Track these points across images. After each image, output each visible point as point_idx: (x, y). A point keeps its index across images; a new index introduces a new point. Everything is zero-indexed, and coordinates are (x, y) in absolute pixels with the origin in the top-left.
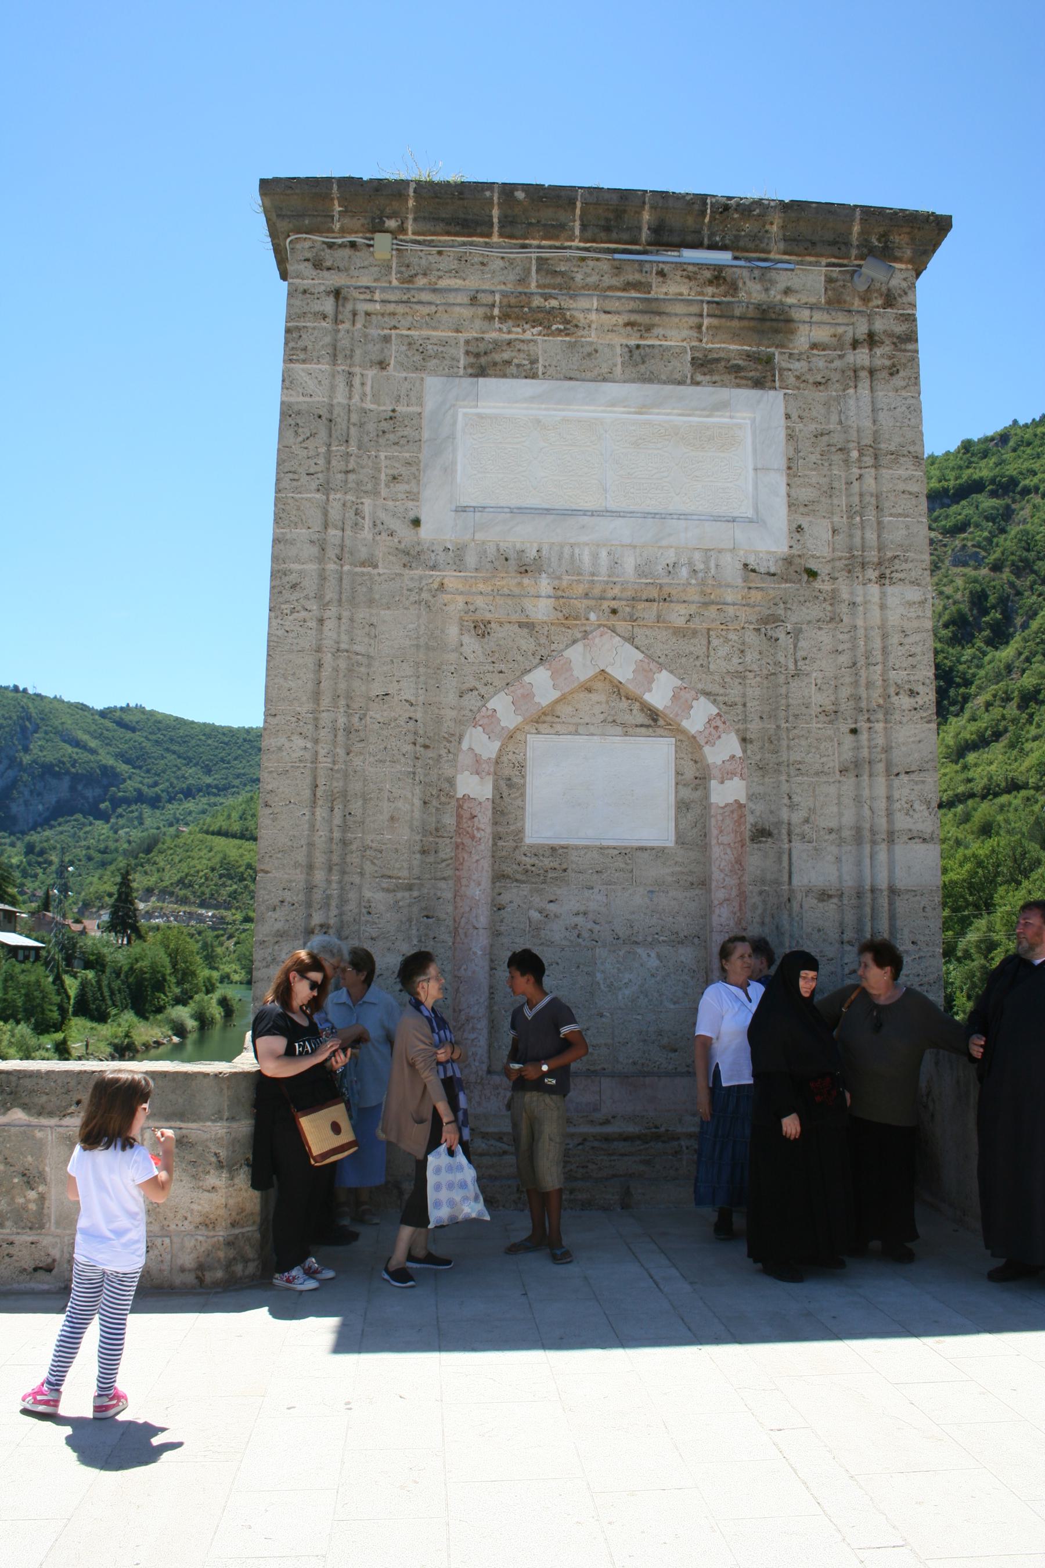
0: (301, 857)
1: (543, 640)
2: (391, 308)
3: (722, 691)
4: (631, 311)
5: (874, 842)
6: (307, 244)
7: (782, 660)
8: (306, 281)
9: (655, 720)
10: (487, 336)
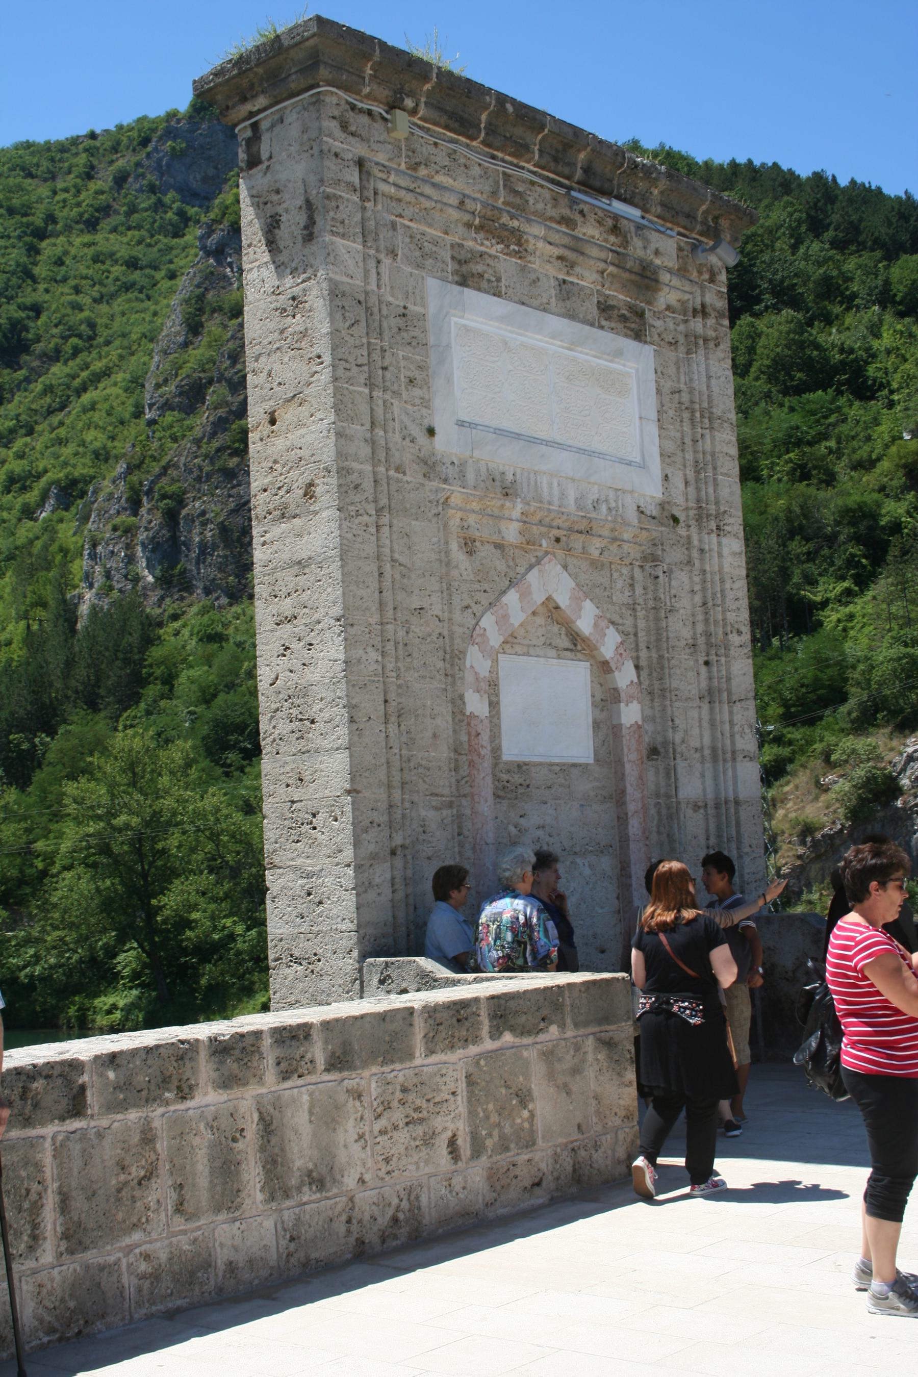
0: (382, 774)
1: (511, 563)
2: (402, 193)
3: (621, 621)
4: (565, 246)
5: (725, 760)
6: (334, 100)
7: (662, 596)
8: (336, 143)
9: (575, 645)
10: (465, 243)
